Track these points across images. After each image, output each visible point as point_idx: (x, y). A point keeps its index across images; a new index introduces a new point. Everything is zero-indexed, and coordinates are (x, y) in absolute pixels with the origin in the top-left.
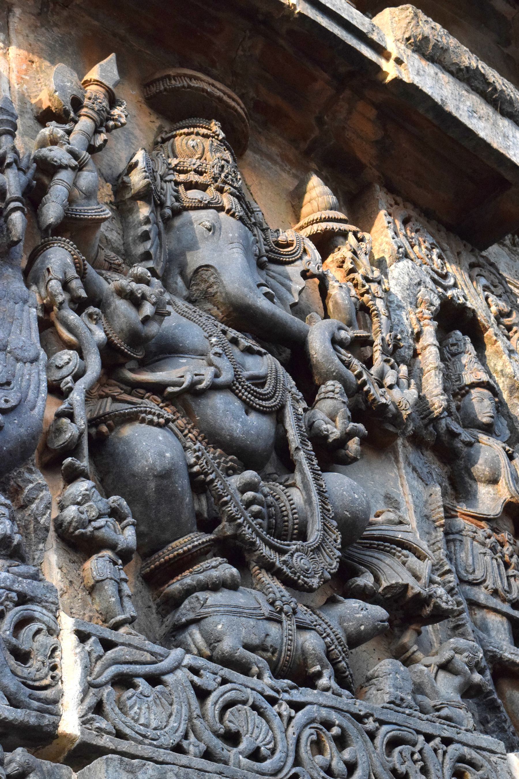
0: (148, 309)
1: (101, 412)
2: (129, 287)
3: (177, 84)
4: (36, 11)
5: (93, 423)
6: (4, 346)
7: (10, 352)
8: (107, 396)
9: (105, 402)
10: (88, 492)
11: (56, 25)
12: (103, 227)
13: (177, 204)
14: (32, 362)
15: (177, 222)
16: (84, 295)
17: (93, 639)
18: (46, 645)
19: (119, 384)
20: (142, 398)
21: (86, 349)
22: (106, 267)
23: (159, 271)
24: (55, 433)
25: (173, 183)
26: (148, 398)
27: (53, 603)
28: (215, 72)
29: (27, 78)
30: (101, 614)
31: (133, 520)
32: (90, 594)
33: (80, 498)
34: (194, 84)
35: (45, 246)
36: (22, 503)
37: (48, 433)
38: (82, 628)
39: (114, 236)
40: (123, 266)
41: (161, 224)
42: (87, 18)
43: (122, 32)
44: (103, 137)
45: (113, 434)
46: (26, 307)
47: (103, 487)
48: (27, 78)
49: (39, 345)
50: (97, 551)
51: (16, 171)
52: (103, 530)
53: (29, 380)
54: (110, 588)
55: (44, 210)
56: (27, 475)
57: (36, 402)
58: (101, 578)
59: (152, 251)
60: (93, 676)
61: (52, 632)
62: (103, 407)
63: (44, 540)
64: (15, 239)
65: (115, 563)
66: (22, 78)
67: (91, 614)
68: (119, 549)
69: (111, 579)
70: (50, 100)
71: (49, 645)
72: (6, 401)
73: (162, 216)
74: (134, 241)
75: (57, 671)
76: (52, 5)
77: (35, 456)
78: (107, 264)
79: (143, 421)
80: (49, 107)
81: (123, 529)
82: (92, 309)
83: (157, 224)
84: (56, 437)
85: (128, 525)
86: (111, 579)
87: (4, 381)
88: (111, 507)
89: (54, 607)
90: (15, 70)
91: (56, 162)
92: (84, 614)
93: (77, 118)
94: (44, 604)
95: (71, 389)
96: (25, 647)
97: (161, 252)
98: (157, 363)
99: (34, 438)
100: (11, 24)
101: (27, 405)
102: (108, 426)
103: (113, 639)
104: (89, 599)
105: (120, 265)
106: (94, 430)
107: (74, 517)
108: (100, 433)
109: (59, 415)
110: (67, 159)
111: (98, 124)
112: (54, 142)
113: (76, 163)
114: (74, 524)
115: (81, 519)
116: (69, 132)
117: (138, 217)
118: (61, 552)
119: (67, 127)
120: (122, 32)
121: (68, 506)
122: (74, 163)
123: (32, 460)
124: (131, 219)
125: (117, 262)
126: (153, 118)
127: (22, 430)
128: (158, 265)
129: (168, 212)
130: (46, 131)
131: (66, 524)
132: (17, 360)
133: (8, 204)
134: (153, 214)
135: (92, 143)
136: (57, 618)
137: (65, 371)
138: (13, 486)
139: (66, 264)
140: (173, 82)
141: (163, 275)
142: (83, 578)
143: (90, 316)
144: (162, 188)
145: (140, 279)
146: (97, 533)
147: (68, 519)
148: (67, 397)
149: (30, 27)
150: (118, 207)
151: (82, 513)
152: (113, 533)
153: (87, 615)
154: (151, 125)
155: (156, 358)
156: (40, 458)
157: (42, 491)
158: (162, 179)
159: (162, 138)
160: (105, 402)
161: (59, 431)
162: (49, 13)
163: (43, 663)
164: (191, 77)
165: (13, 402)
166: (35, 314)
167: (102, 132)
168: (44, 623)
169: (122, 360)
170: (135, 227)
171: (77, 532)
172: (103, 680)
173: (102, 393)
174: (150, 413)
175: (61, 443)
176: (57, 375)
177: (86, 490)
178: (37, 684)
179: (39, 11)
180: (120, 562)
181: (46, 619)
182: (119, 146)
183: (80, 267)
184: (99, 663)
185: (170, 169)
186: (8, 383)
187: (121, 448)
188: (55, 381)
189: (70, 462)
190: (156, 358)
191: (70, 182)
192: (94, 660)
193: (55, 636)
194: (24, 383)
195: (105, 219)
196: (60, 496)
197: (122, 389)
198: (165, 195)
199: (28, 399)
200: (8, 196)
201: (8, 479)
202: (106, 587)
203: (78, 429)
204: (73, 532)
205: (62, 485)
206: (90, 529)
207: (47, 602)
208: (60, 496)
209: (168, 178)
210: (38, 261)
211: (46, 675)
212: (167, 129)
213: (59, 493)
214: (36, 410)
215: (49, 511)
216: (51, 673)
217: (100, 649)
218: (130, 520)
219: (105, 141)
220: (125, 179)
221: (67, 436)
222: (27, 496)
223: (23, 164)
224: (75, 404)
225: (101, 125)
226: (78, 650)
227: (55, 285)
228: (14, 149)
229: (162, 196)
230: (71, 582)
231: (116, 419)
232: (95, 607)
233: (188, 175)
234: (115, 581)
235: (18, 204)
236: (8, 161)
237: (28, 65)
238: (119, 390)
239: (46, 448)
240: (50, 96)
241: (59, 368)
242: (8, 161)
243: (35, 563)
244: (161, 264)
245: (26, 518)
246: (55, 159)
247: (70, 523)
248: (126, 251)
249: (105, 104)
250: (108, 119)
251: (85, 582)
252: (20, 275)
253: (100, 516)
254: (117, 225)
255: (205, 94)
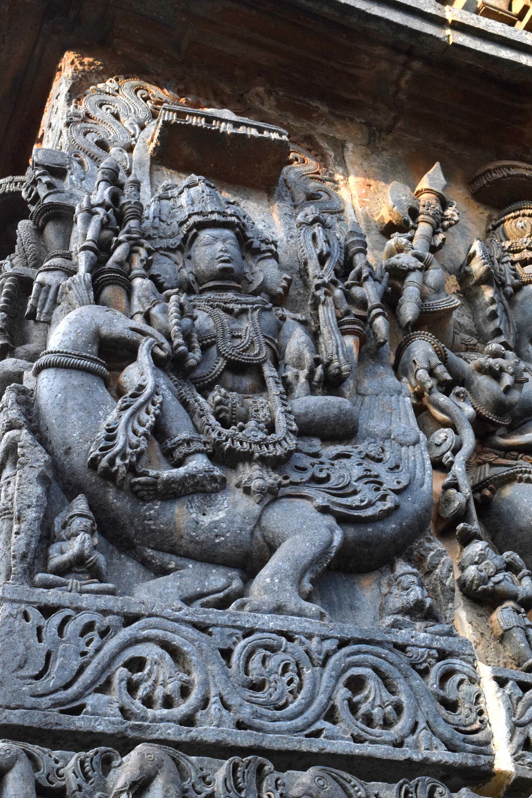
0: (507, 380)
1: (482, 478)
2: (487, 364)
3: (498, 175)
4: (365, 141)
5: (476, 488)
6: (388, 435)
7: (394, 439)
8: (484, 463)
9: (483, 469)
10: (483, 552)
11: (384, 149)
12: (455, 315)
13: (516, 281)
14: (414, 444)
15: (520, 297)
16: (449, 378)
17: (510, 683)
18: (470, 693)
19: (493, 450)
20: (516, 459)
21: (458, 425)
22: (463, 349)
23: (511, 344)
24: (445, 503)
25: (509, 263)
26: (521, 458)
27: (469, 655)
28: (529, 157)
29: (368, 200)
30: (514, 659)
31: (528, 571)
32: (501, 642)
33: (477, 558)
34: (513, 172)
35: (408, 342)
36: (427, 570)
37: (438, 504)
38: (499, 675)
39: (465, 321)
40: (478, 345)
41: (505, 302)
42: (410, 137)
43: (441, 141)
44: (441, 236)
45: (496, 496)
46: (401, 397)
47: (495, 544)
48: (368, 200)
49: (417, 429)
50: (501, 604)
51: (373, 282)
52: (503, 584)
53: (415, 460)
54: (518, 635)
55: (402, 310)
56: (427, 545)
57: (424, 479)
58: (508, 627)
59: (502, 327)
60: (517, 717)
61: (473, 681)
62: (483, 474)
63: (452, 600)
64: (382, 341)
65: (519, 612)
66: (363, 201)
67: (505, 661)
68: (519, 599)
69: (518, 627)
70: (390, 215)
71: (473, 693)
72: (398, 483)
73: (505, 294)
74: (484, 321)
75: (484, 716)
76: (377, 133)
77: (431, 526)
78: (464, 346)
79: (521, 480)
80: (390, 221)
81: (520, 580)
82: (458, 389)
83: (502, 302)
84: (446, 507)
85: (524, 576)
86: (518, 627)
87: (394, 465)
88: (506, 562)
89: (471, 659)
90: (357, 196)
91: (405, 267)
92: (499, 661)
93: (416, 226)
94: (462, 657)
95: (452, 463)
96: (452, 697)
97: (509, 327)
98: (524, 426)
99: (427, 511)
100: (346, 158)
101: (417, 483)
102: (491, 490)
103: (529, 681)
104: (500, 647)
105: (475, 345)
106: (478, 495)
107: (475, 576)
108: (484, 497)
109: (446, 487)
110: (414, 263)
111: (435, 227)
112: (400, 250)
113: (422, 264)
114: (475, 582)
115: (481, 577)
116: (411, 239)
117: (484, 299)
118: (468, 608)
119: (409, 234)
120: (441, 141)
121: (467, 566)
122: (420, 264)
123: (430, 531)
124: (477, 302)
125: (472, 342)
126: (482, 210)
127: (416, 506)
128: (508, 338)
129: (510, 289)
130: (391, 243)
131: (468, 583)
132: (402, 445)
133: (370, 312)
134: (496, 295)
135: (433, 244)
136: (475, 668)
137: (444, 448)
138: (416, 556)
139: (428, 354)
140: (494, 174)
141: (515, 347)
142: (492, 629)
143: (457, 395)
144: (501, 270)
145: (495, 355)
146: (497, 587)
147: (470, 578)
148: (450, 470)
149: (362, 156)
150: (464, 294)
151: (481, 571)
152: (511, 585)
153: (501, 662)
154: (480, 215)
155: (522, 421)
156: (436, 527)
157: (442, 557)
158: (499, 262)
159: (492, 225)
160: (483, 469)
161: (448, 501)
162: (377, 140)
163: (471, 709)
164: (509, 167)
165: (404, 483)
166: (409, 402)
167: (439, 232)
168: (465, 674)
169: (492, 429)
170: (483, 309)
171: (480, 589)
172: (527, 719)
173: (480, 461)
174: (526, 472)
175: (452, 511)
176: (438, 452)
177: (481, 550)
178: (468, 729)
179: (367, 141)
180: (523, 610)
181: (466, 670)
182: (456, 241)
183: (441, 354)
184: (521, 705)
185: (505, 252)
186: (397, 467)
187: (505, 507)
188: (437, 457)
189: (463, 527)
190: (522, 421)
191: (420, 282)
192: (515, 702)
193: (477, 684)
194: (411, 465)
195: (455, 308)
196: (458, 558)
197: (496, 454)
198: (504, 276)
199: (417, 477)
200: (370, 305)
201: (412, 550)
202: (514, 635)
203: (465, 497)
204: (476, 589)
205: (459, 548)
206: (491, 584)
207: (464, 654)
208: (458, 558)
209: (504, 260)
210: (404, 355)
211: (475, 720)
212: (495, 217)
213: (458, 556)
214: (425, 486)
215: (452, 574)
216: (479, 718)
217: (518, 691)
218: (525, 571)
219: (444, 240)
220: (467, 268)
221: (456, 505)
222: (430, 563)
223: (377, 275)
224: (459, 475)
225: (438, 227)
226: (500, 694)
227: (423, 374)
228: (367, 264)
229: (502, 277)
230: (482, 634)
231: (497, 482)
232: (507, 653)
233: (522, 253)
234: (521, 628)
235: (379, 310)
236: (364, 275)
237: (366, 189)
238: (495, 456)
239: (439, 518)
240: (390, 211)
241: (438, 445)
242: (364, 275)
243: (448, 622)
244: (512, 337)
245: (433, 582)
246: (404, 265)
247: (472, 582)
248: (478, 331)
249: (438, 207)
250: (443, 220)
251: (495, 632)
252: (390, 371)
253: (498, 571)
254: (466, 310)
255: (524, 179)
